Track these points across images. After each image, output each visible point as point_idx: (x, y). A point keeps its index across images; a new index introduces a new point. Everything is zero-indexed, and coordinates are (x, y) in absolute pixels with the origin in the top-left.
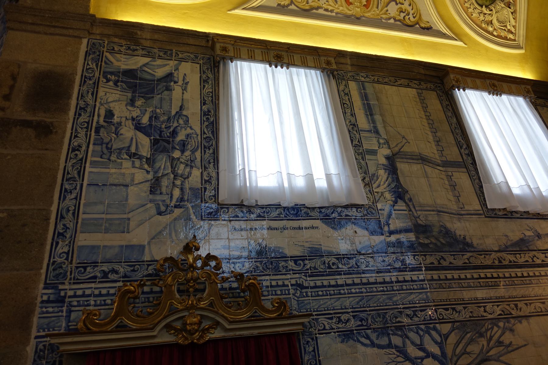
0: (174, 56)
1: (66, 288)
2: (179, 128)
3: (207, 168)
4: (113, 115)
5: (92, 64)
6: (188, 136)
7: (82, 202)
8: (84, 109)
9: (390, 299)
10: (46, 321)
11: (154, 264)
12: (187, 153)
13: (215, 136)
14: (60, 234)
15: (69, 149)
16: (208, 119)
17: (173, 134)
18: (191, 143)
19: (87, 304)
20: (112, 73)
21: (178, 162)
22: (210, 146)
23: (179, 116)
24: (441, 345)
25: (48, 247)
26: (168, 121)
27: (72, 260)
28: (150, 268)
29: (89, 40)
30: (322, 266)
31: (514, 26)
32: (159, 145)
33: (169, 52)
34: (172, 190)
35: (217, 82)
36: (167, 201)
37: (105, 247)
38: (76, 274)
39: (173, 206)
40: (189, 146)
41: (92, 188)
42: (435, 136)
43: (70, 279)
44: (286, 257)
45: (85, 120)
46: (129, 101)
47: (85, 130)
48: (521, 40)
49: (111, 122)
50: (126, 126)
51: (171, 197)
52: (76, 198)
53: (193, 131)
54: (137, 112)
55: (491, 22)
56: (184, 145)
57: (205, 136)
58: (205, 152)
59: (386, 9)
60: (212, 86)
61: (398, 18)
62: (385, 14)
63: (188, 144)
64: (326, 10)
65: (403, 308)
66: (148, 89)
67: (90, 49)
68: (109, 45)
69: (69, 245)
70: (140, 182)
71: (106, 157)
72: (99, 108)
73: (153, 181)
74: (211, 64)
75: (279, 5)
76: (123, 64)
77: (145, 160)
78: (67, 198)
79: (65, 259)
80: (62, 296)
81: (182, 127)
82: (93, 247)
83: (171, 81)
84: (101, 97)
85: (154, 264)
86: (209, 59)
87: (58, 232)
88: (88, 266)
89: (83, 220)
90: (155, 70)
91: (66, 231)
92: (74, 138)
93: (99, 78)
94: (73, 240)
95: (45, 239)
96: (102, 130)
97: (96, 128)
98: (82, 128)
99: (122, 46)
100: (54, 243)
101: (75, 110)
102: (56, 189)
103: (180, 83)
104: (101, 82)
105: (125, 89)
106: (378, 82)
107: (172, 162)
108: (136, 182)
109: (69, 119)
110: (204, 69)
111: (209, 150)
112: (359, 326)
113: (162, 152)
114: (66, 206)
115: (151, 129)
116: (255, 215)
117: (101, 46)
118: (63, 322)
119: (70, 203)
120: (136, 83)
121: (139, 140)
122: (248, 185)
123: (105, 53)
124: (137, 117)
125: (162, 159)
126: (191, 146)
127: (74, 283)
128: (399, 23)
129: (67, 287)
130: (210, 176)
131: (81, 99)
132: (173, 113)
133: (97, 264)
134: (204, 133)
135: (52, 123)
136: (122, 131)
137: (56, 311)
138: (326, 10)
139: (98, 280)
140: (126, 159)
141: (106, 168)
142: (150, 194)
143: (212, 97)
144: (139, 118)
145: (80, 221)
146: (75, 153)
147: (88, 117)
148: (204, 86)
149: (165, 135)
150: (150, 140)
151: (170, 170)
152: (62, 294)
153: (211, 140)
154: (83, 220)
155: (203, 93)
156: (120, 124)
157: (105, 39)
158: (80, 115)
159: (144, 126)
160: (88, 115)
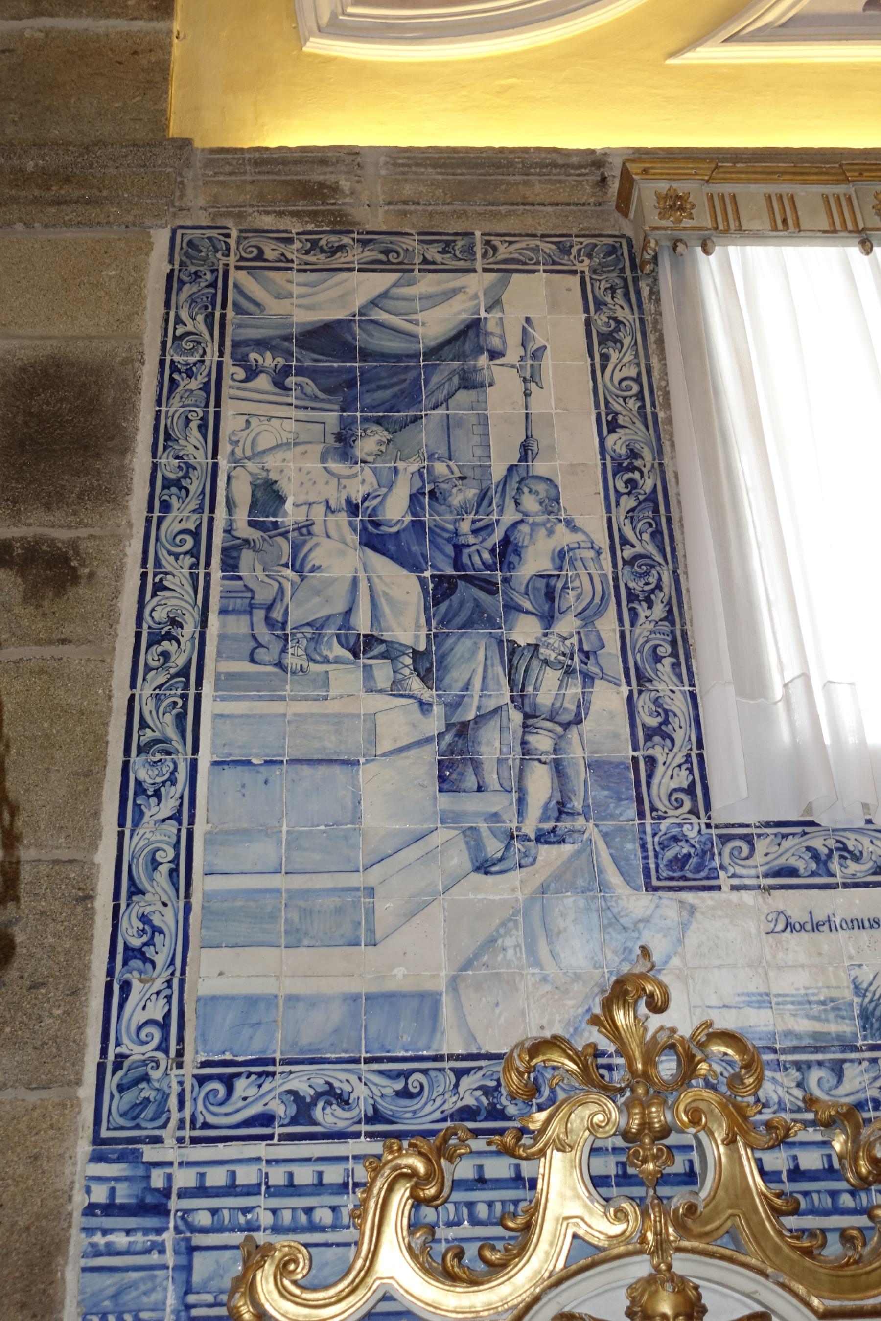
0: (479, 256)
1: (168, 1159)
2: (525, 529)
3: (650, 681)
4: (280, 499)
5: (194, 319)
6: (561, 556)
7: (200, 830)
8: (177, 483)
10: (109, 1282)
11: (480, 1068)
12: (567, 625)
13: (668, 549)
14: (132, 953)
15: (138, 635)
16: (632, 484)
17: (503, 555)
18: (577, 583)
19: (248, 1222)
20: (262, 344)
21: (535, 664)
22: (653, 591)
23: (522, 480)
25: (96, 1003)
26: (479, 505)
27: (180, 1053)
28: (467, 1082)
29: (174, 232)
32: (455, 598)
33: (460, 243)
34: (521, 771)
35: (652, 337)
36: (505, 817)
37: (293, 999)
38: (200, 1107)
39: (533, 837)
40: (572, 594)
41: (230, 774)
43: (181, 1125)
45: (183, 526)
46: (331, 440)
47: (189, 560)
49: (275, 525)
50: (328, 536)
51: (521, 801)
52: (176, 817)
53: (579, 537)
54: (363, 481)
56: (550, 595)
57: (628, 553)
58: (634, 615)
60: (637, 356)
63: (565, 587)
66: (396, 389)
67: (182, 264)
68: (245, 243)
69: (168, 992)
70: (399, 744)
71: (267, 658)
72: (229, 478)
73: (448, 738)
74: (622, 270)
76: (299, 306)
77: (408, 661)
78: (146, 818)
79: (157, 1049)
80: (157, 1190)
81: (534, 525)
82: (252, 1002)
83: (479, 350)
84: (233, 433)
85: (480, 1068)
86: (613, 250)
87: (127, 947)
88: (238, 1075)
89: (208, 897)
90: (414, 317)
91: (150, 943)
92: (154, 595)
93: (220, 365)
94: (178, 973)
95: (84, 973)
96: (246, 557)
97: (224, 550)
98: (177, 556)
99: (289, 241)
100: (116, 988)
101: (147, 490)
102: (106, 786)
103: (513, 354)
104: (226, 382)
105: (316, 398)
107: (510, 661)
108: (385, 745)
109: (130, 525)
110: (600, 293)
111: (650, 607)
113: (468, 624)
114: (147, 845)
115: (422, 543)
117: (217, 251)
118: (165, 1289)
119: (158, 837)
120: (352, 370)
121: (379, 587)
122: (827, 740)
123: (233, 274)
124: (364, 499)
125: (474, 652)
126: (578, 597)
127: (195, 1141)
129: (168, 1152)
130: (666, 712)
131: (165, 448)
132: (498, 472)
133: (270, 1069)
134: (625, 541)
135: (74, 544)
136: (315, 558)
137: (139, 1247)
139: (278, 1131)
140: (338, 661)
141: (272, 699)
142: (440, 791)
143: (640, 396)
144: (375, 502)
145: (196, 900)
146: (160, 649)
147: (194, 511)
148: (605, 358)
149: (476, 559)
150: (422, 582)
151: (508, 694)
152: (157, 1180)
153: (653, 566)
154: (208, 897)
155: (605, 386)
156: (306, 529)
157: (230, 223)
158: (166, 507)
159: (394, 530)
160: (194, 504)
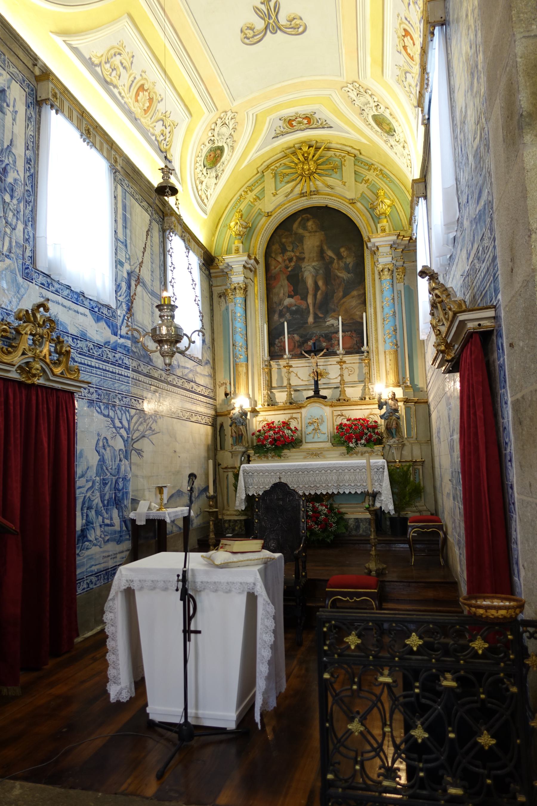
9: (113, 384)
12: (15, 201)
24: (129, 422)
30: (86, 348)
31: (211, 194)
42: (152, 267)
44: (68, 333)
48: (209, 209)
55: (202, 183)
59: (155, 124)
61: (158, 138)
62: (153, 128)
64: (120, 93)
65: (118, 393)
75: (90, 59)
106: (133, 196)
112: (98, 399)
116: (54, 289)
128: (156, 143)
138: (120, 93)
143: (33, 142)
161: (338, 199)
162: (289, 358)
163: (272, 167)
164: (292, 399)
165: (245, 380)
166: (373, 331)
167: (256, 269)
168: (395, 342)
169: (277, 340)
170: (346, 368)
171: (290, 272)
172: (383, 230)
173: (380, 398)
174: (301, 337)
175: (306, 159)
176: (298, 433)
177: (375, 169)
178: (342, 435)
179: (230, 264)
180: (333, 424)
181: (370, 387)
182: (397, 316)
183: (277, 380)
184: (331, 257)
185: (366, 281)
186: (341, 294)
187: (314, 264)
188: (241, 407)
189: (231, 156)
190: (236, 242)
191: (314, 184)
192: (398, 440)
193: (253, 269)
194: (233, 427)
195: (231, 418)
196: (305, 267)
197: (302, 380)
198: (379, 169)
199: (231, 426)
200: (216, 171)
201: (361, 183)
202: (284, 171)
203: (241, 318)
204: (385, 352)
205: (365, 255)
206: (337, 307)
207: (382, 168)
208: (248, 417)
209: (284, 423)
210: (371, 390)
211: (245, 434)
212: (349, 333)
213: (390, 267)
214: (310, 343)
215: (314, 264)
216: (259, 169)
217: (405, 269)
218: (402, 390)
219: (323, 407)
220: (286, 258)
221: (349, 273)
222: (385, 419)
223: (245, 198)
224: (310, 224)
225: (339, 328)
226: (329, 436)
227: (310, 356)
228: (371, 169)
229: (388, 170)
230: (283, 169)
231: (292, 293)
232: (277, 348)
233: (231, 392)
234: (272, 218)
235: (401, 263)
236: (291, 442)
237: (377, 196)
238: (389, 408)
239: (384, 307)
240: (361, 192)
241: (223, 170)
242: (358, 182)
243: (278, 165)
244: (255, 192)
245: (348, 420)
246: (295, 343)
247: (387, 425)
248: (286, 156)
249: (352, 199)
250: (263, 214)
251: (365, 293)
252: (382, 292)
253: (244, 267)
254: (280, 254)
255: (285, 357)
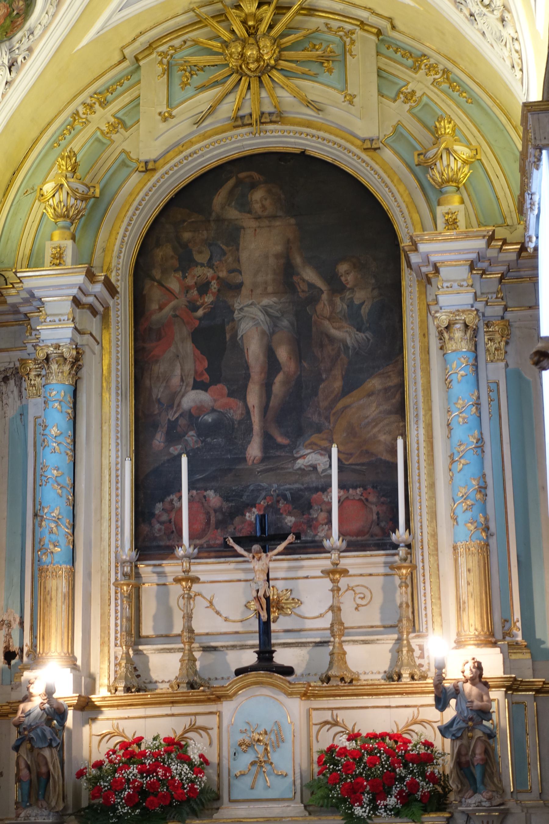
161: (333, 138)
162: (189, 557)
163: (161, 49)
164: (196, 673)
165: (65, 614)
166: (424, 490)
167: (107, 308)
168: (482, 520)
169: (159, 506)
170: (349, 588)
171: (200, 319)
172: (452, 224)
173: (439, 679)
174: (226, 498)
175: (252, 32)
176: (211, 771)
177: (431, 68)
178: (335, 780)
179: (37, 293)
180: (310, 749)
181: (414, 643)
182: (487, 448)
183: (155, 618)
184: (311, 286)
185: (405, 352)
186: (338, 384)
187: (265, 301)
188: (49, 693)
189: (54, 15)
190: (57, 235)
191: (271, 96)
192: (489, 799)
193: (101, 309)
194: (23, 751)
195: (18, 725)
196: (241, 309)
197: (226, 619)
198: (441, 67)
199: (16, 748)
200: (11, 51)
201: (395, 100)
202: (194, 59)
203: (59, 439)
204: (455, 548)
205: (404, 283)
206: (327, 418)
207: (450, 66)
208: (69, 722)
209: (169, 741)
210: (417, 653)
211: (56, 773)
212: (359, 491)
213: (470, 318)
214: (251, 516)
215: (265, 301)
216: (127, 51)
217: (508, 325)
218: (501, 656)
219: (282, 698)
220: (190, 281)
221: (359, 330)
222: (455, 738)
223: (87, 122)
224: (258, 195)
225: (330, 476)
226: (298, 782)
227: (249, 551)
228: (419, 67)
229: (462, 71)
230: (191, 55)
231: (206, 378)
232: (157, 526)
233: (22, 650)
234: (157, 175)
235: (498, 310)
236: (188, 800)
237: (435, 133)
238: (464, 706)
239: (454, 425)
240: (394, 123)
241: (30, 50)
242: (387, 98)
243: (177, 42)
244: (114, 107)
245: (352, 737)
246: (208, 514)
247: (459, 754)
248: (198, 23)
249: (372, 140)
250: (134, 165)
251: (401, 386)
252: (447, 383)
253: (76, 302)
254: (176, 271)
255: (180, 552)
